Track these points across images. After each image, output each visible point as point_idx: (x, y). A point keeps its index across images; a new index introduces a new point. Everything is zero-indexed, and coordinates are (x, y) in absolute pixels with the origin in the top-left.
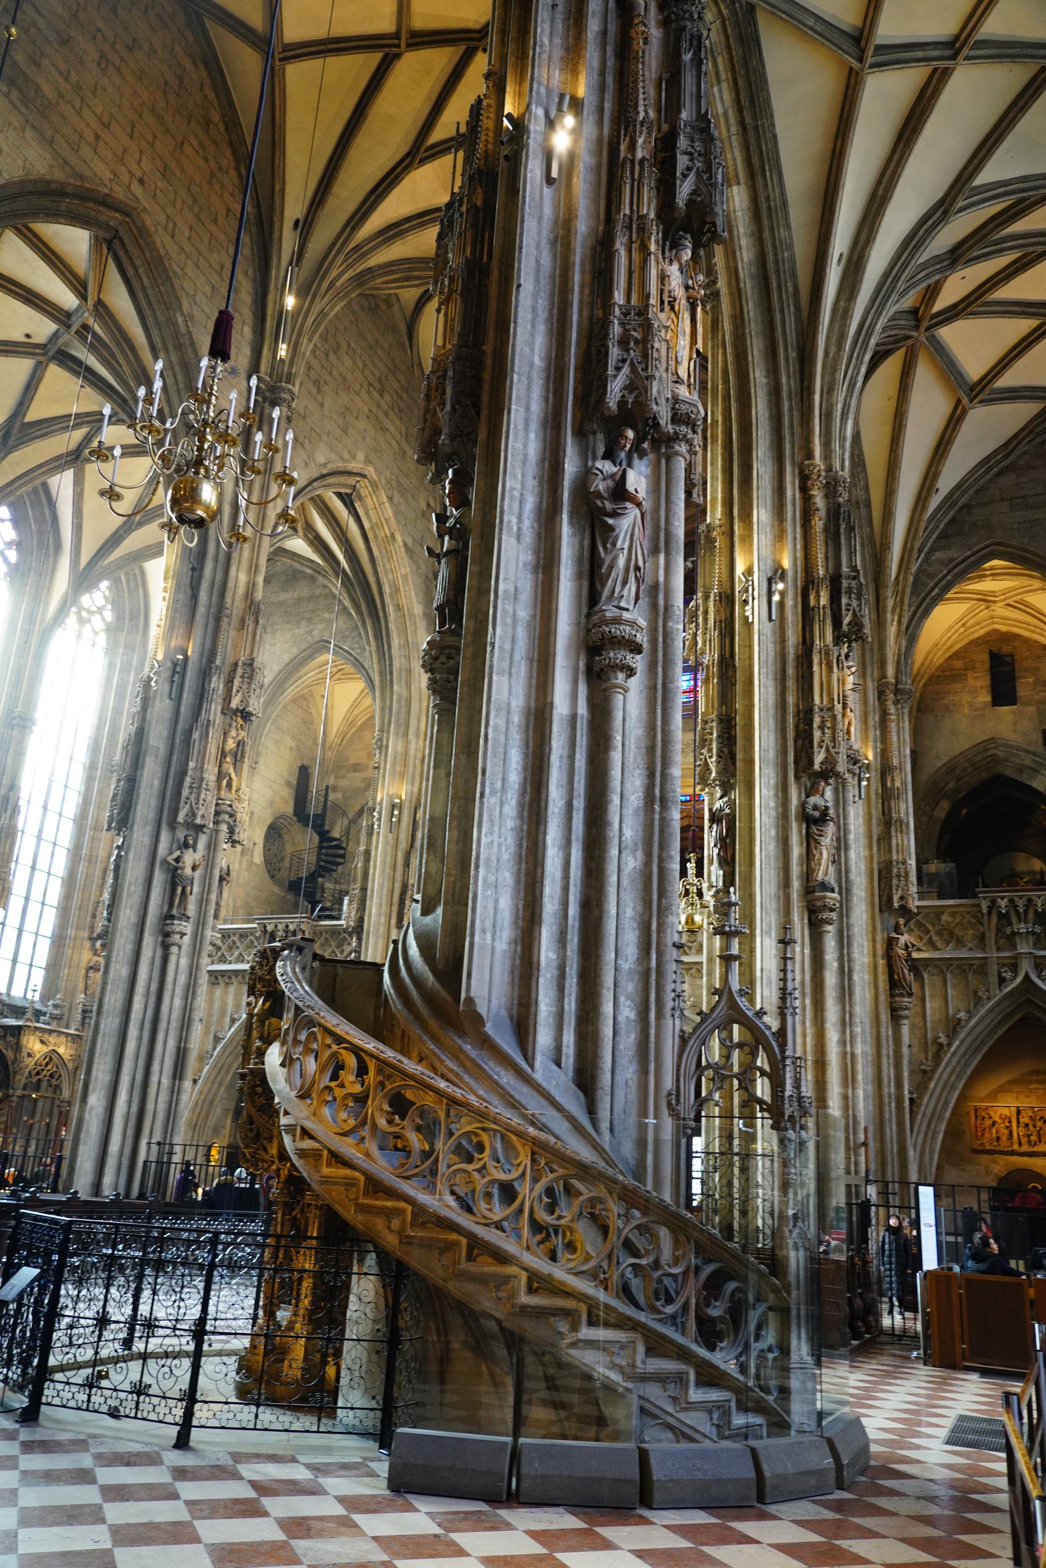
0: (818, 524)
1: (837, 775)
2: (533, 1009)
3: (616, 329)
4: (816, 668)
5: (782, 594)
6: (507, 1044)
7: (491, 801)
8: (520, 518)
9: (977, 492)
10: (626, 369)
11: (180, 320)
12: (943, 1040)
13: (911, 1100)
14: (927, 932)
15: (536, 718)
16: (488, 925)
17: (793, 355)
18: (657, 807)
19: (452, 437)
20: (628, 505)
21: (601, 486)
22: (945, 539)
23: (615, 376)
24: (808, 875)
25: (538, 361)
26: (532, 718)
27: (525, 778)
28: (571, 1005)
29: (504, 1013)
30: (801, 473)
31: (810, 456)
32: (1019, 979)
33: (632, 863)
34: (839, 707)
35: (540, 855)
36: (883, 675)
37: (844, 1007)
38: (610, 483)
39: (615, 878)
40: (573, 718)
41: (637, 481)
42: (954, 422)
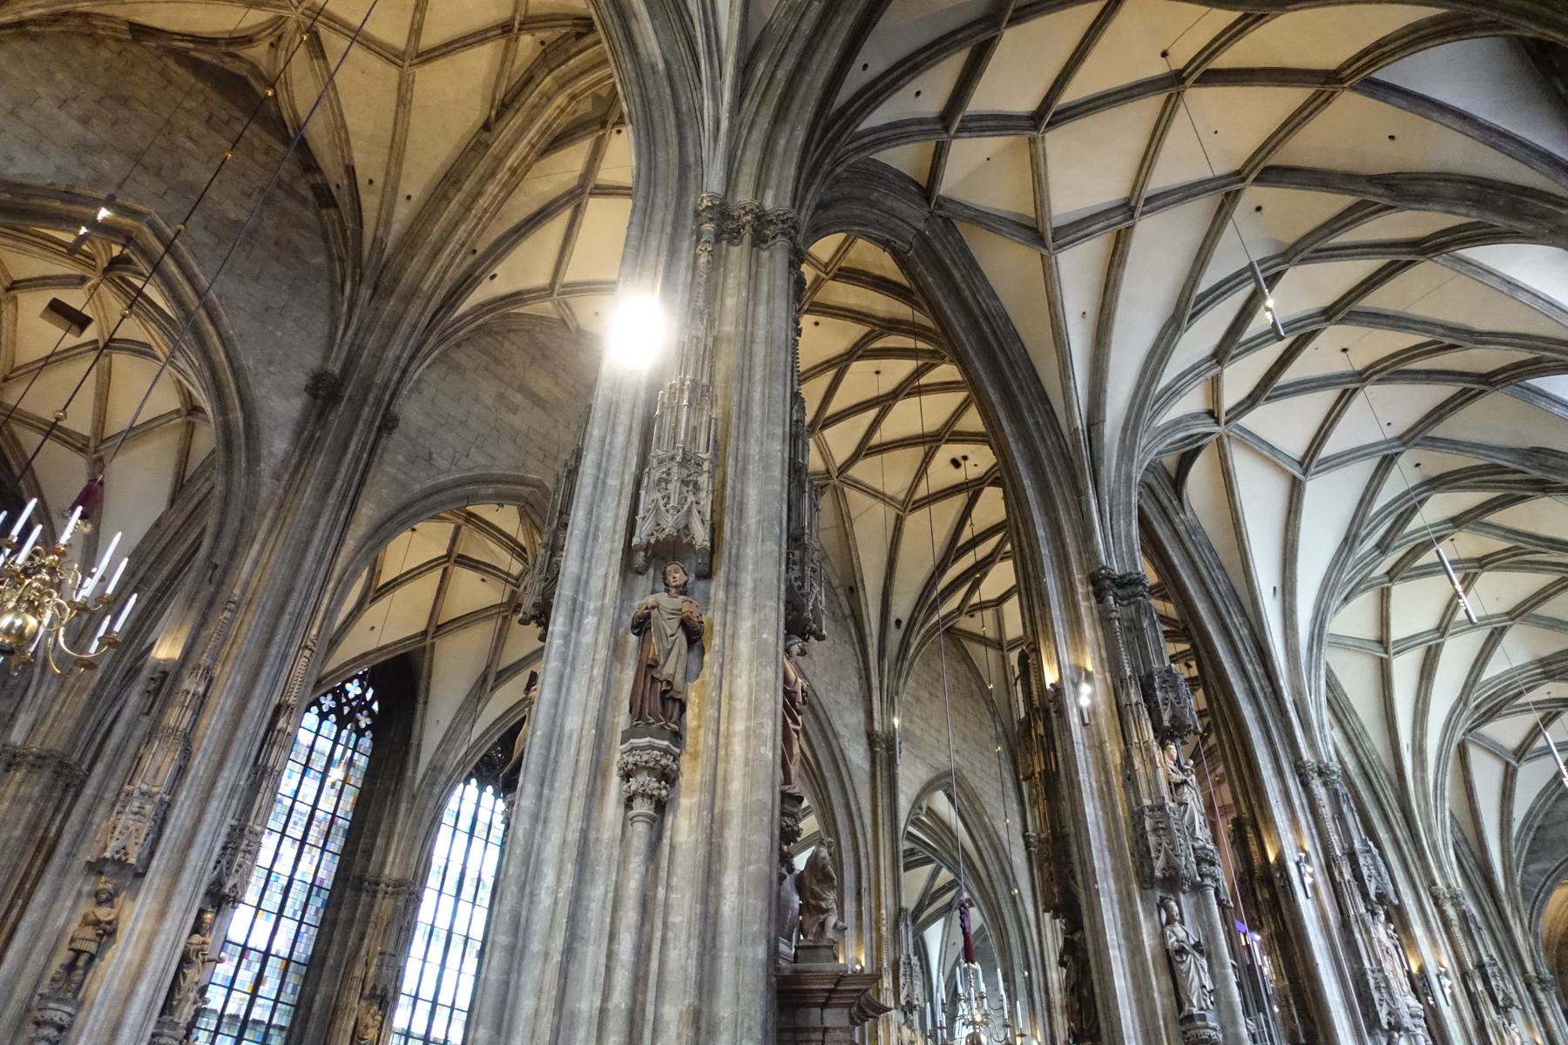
0: (1456, 930)
3: (1372, 982)
5: (1451, 987)
9: (1546, 815)
11: (987, 820)
17: (1399, 815)
22: (1533, 854)
30: (1432, 895)
31: (1434, 883)
36: (1524, 971)
42: (1509, 776)
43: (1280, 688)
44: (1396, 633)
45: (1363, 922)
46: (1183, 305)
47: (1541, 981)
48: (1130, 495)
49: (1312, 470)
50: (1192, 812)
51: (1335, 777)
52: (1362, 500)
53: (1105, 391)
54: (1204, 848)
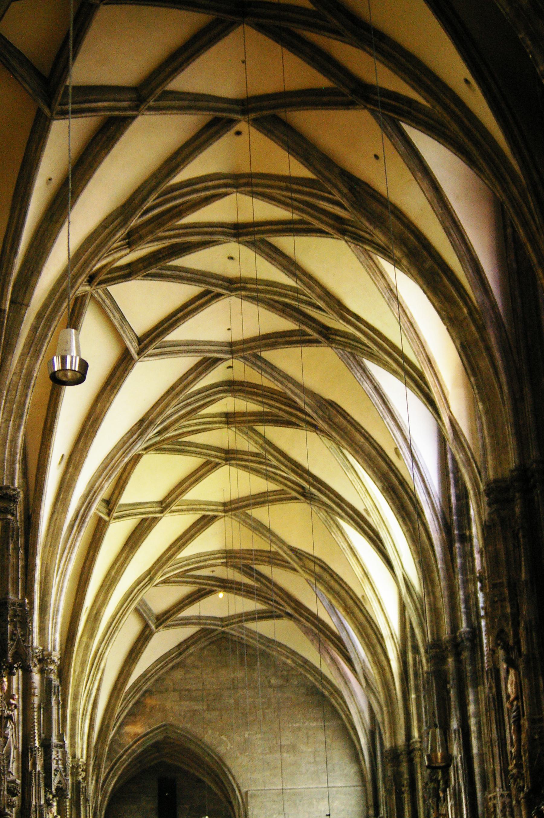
9: (157, 680)
43: (34, 565)
44: (127, 498)
46: (137, 201)
48: (26, 396)
49: (150, 351)
50: (10, 747)
51: (52, 667)
52: (172, 388)
53: (39, 273)
54: (14, 782)
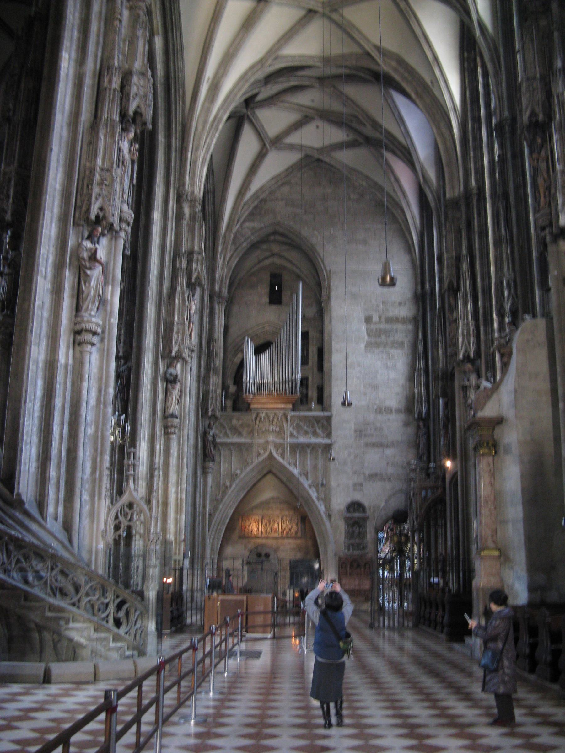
1: (184, 359)
2: (46, 498)
4: (177, 301)
6: (34, 512)
7: (29, 405)
8: (46, 268)
10: (100, 200)
12: (228, 484)
13: (210, 515)
14: (225, 428)
15: (50, 365)
16: (27, 461)
18: (102, 406)
19: (12, 215)
20: (97, 264)
21: (85, 255)
22: (252, 216)
23: (95, 203)
24: (165, 409)
25: (58, 187)
26: (48, 365)
27: (44, 393)
28: (62, 495)
29: (33, 499)
32: (267, 454)
33: (90, 431)
34: (187, 322)
35: (50, 430)
37: (178, 476)
38: (90, 254)
39: (83, 439)
40: (66, 365)
41: (101, 255)
45: (112, 126)
47: (220, 296)
